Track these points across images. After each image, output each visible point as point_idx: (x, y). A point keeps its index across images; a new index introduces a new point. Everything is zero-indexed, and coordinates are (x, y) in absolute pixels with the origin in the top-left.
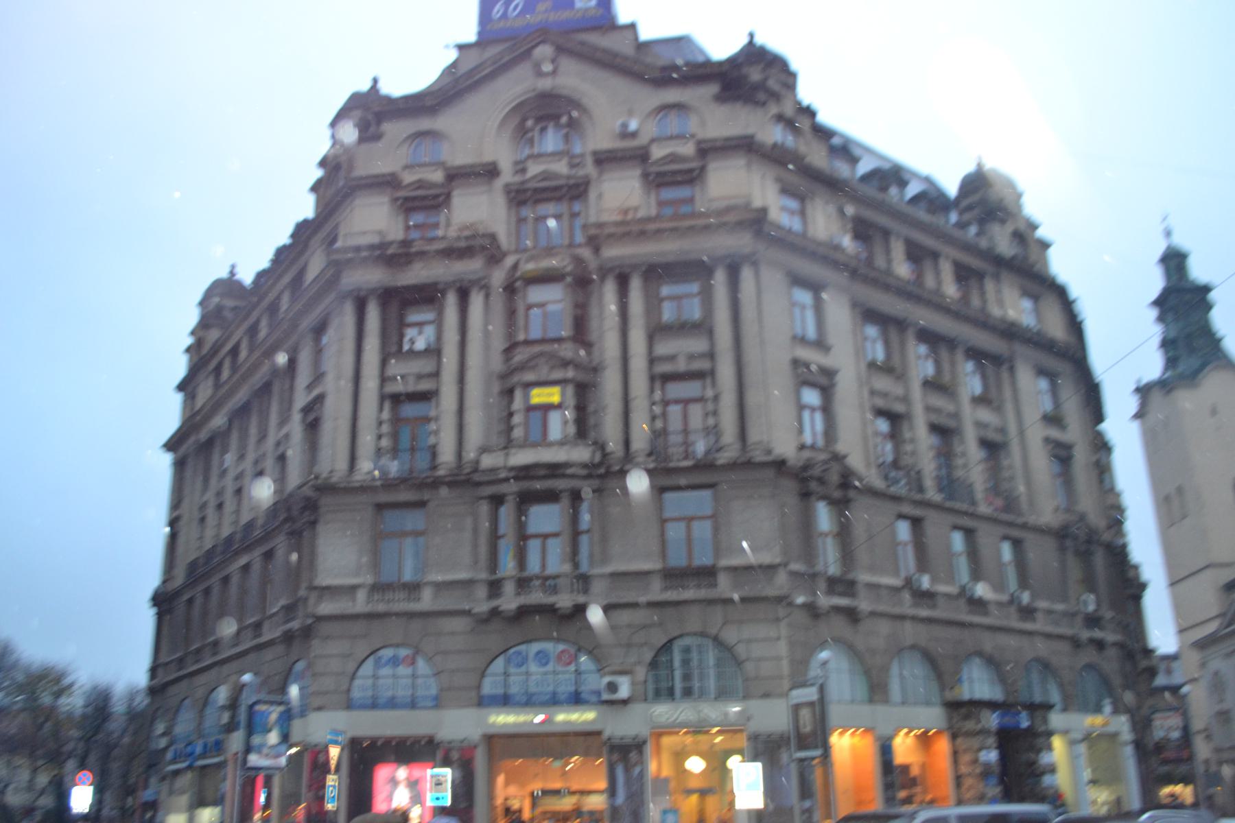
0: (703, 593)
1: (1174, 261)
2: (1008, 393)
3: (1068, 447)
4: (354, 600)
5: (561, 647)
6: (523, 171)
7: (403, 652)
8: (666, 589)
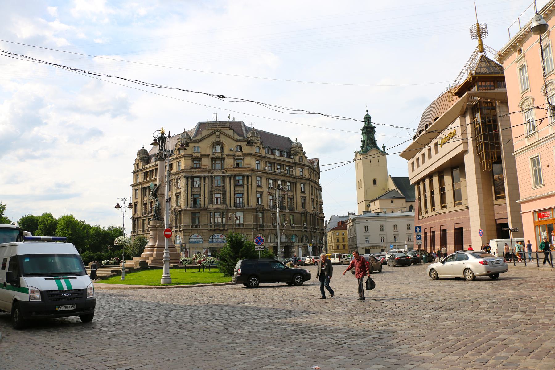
0: (241, 228)
1: (368, 118)
2: (295, 189)
3: (305, 197)
4: (189, 227)
5: (221, 235)
6: (214, 155)
7: (197, 235)
8: (236, 227)
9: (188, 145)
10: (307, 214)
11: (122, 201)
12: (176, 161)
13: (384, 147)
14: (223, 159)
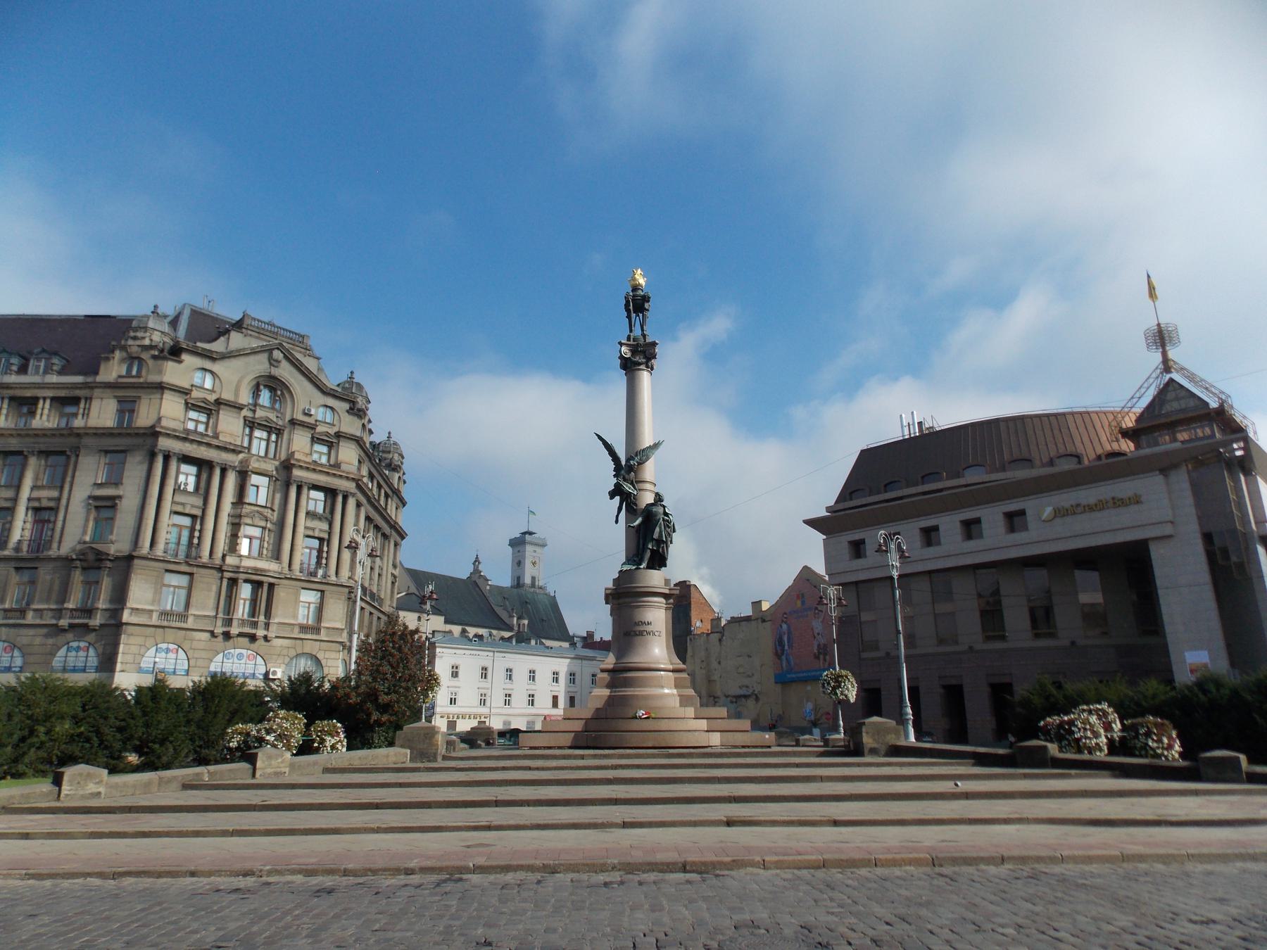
0: (314, 637)
4: (151, 617)
5: (250, 652)
6: (254, 411)
7: (172, 646)
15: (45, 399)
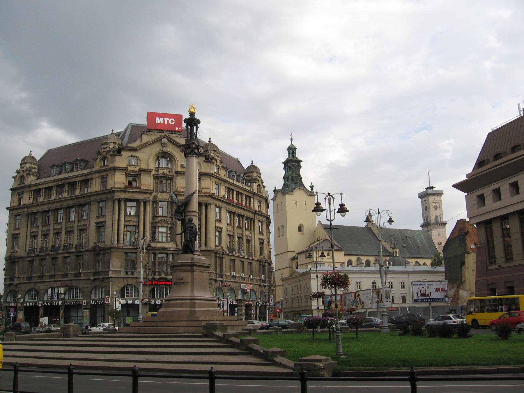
3: (263, 240)
4: (121, 274)
6: (158, 171)
9: (121, 153)
10: (265, 263)
11: (325, 199)
12: (97, 175)
13: (312, 187)
14: (171, 178)
15: (78, 181)
